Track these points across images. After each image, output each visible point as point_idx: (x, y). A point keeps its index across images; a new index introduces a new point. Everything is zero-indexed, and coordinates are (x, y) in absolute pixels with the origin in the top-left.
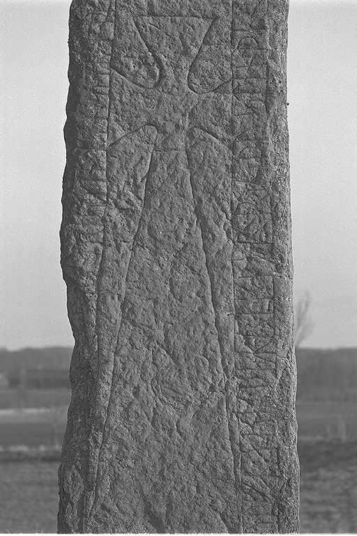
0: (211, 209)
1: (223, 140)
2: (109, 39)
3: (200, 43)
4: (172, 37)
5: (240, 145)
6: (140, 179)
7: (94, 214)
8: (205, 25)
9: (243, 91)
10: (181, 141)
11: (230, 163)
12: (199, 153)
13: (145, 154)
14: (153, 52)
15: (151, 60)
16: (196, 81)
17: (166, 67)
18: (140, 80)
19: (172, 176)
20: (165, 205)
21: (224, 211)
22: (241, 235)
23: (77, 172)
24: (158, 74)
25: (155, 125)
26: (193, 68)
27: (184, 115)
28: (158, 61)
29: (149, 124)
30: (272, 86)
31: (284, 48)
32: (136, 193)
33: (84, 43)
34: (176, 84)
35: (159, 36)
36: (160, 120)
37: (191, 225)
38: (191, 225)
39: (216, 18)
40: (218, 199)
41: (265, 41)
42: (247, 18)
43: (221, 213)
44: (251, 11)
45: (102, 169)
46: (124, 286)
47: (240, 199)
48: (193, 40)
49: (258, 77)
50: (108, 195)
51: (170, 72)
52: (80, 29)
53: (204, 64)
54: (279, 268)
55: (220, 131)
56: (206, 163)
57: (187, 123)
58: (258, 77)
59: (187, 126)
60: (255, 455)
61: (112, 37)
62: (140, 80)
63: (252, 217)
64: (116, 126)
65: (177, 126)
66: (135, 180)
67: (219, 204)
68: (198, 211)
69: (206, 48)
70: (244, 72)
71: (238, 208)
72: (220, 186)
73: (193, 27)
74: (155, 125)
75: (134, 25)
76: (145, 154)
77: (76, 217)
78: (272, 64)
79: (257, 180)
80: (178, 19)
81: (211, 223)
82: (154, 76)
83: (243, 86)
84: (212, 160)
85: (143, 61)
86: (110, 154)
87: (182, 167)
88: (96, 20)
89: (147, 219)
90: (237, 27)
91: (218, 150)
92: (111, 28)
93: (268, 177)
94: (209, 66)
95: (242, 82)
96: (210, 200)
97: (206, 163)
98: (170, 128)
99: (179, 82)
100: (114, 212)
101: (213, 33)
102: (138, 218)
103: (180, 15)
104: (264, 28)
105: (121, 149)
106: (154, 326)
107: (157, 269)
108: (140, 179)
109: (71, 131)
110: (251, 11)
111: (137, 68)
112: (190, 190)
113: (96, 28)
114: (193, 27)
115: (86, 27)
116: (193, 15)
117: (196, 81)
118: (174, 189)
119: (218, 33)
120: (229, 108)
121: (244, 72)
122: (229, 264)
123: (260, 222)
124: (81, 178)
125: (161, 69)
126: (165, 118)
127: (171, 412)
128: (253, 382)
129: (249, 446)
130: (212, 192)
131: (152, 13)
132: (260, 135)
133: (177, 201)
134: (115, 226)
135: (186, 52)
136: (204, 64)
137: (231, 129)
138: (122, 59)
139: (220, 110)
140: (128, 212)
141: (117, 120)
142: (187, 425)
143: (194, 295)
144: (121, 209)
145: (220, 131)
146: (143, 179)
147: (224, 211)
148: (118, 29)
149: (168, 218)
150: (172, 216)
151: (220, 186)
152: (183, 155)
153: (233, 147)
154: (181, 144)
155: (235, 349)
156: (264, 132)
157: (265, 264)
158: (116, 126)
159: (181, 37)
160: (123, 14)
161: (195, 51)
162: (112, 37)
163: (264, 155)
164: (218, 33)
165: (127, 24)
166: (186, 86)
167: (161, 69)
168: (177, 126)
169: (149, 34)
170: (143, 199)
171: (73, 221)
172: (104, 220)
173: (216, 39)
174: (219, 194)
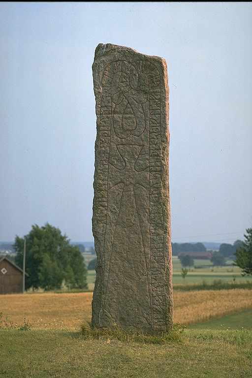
12: (138, 192)
15: (122, 160)
21: (147, 212)
22: (151, 220)
31: (168, 156)
46: (113, 238)
48: (136, 153)
53: (140, 161)
54: (165, 233)
60: (157, 298)
64: (110, 183)
69: (140, 156)
80: (131, 146)
81: (142, 217)
94: (141, 162)
106: (123, 253)
107: (124, 233)
122: (148, 231)
127: (129, 283)
128: (157, 272)
129: (155, 295)
130: (142, 206)
142: (134, 288)
143: (136, 242)
147: (147, 212)
155: (150, 261)
157: (161, 232)
166: (134, 170)
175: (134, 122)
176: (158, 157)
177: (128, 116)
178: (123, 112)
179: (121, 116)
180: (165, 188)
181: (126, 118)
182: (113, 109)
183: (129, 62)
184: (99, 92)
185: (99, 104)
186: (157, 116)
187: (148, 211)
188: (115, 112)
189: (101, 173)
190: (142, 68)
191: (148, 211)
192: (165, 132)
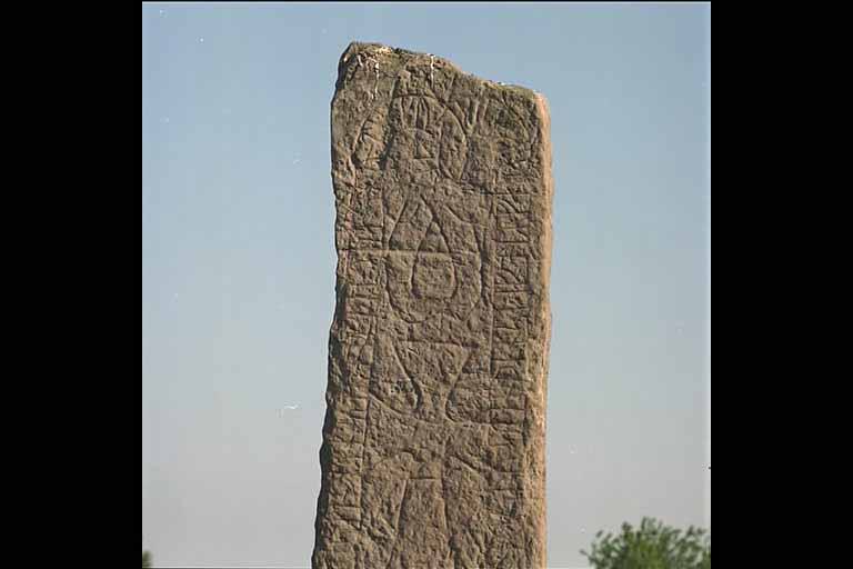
0: (465, 541)
1: (480, 470)
2: (367, 364)
3: (459, 370)
4: (430, 363)
5: (496, 475)
6: (394, 506)
7: (346, 541)
8: (465, 351)
9: (499, 422)
10: (436, 468)
11: (485, 494)
12: (454, 482)
13: (399, 481)
14: (412, 378)
16: (454, 409)
17: (423, 394)
18: (398, 406)
19: (427, 505)
20: (418, 535)
21: (477, 543)
23: (331, 497)
24: (416, 400)
25: (411, 451)
26: (451, 396)
27: (440, 443)
28: (416, 387)
29: (405, 451)
30: (530, 418)
32: (389, 521)
33: (342, 364)
34: (434, 411)
35: (418, 362)
36: (416, 447)
37: (444, 557)
38: (444, 557)
39: (475, 345)
40: (470, 531)
41: (524, 372)
42: (506, 347)
43: (475, 546)
44: (512, 340)
45: (356, 494)
47: (494, 532)
48: (452, 367)
49: (515, 407)
50: (361, 523)
51: (427, 398)
52: (340, 353)
53: (462, 391)
55: (476, 461)
56: (462, 493)
57: (444, 451)
58: (515, 407)
59: (443, 456)
61: (371, 360)
62: (398, 406)
63: (505, 551)
64: (372, 451)
65: (433, 454)
66: (389, 505)
67: (473, 535)
68: (451, 543)
70: (502, 401)
71: (492, 542)
72: (475, 518)
73: (453, 355)
74: (411, 451)
75: (393, 349)
76: (399, 481)
77: (329, 544)
78: (530, 394)
79: (513, 513)
80: (438, 345)
81: (464, 555)
82: (411, 402)
83: (501, 416)
84: (467, 490)
85: (402, 387)
86: (365, 479)
87: (437, 496)
88: (356, 343)
89: (400, 549)
90: (496, 357)
91: (473, 480)
92: (369, 351)
93: (523, 511)
95: (499, 412)
96: (464, 532)
97: (462, 493)
98: (426, 455)
99: (436, 409)
100: (367, 541)
101: (473, 361)
102: (390, 546)
103: (441, 342)
104: (523, 358)
105: (376, 475)
108: (394, 506)
109: (326, 454)
110: (512, 340)
111: (395, 393)
112: (443, 519)
113: (356, 350)
114: (453, 355)
115: (345, 350)
116: (454, 343)
117: (454, 409)
118: (428, 519)
119: (478, 362)
120: (485, 437)
121: (502, 401)
123: (514, 557)
124: (335, 504)
125: (420, 395)
126: (422, 447)
130: (467, 523)
131: (411, 339)
132: (516, 467)
133: (430, 530)
134: (367, 555)
135: (445, 381)
136: (462, 391)
137: (488, 459)
138: (380, 383)
139: (477, 441)
140: (381, 541)
141: (373, 446)
144: (374, 538)
145: (476, 461)
146: (397, 507)
147: (477, 543)
148: (377, 352)
149: (421, 550)
150: (425, 547)
151: (475, 518)
152: (438, 483)
153: (489, 478)
154: (436, 473)
156: (520, 465)
158: (372, 451)
159: (441, 364)
160: (382, 338)
161: (453, 378)
162: (371, 360)
163: (520, 488)
164: (478, 362)
165: (386, 348)
166: (444, 416)
167: (420, 395)
168: (433, 454)
169: (408, 359)
170: (396, 527)
171: (325, 547)
172: (356, 548)
173: (474, 367)
174: (473, 526)
175: (448, 277)
176: (517, 382)
177: (430, 256)
178: (416, 244)
179: (410, 256)
180: (534, 475)
181: (424, 263)
182: (388, 237)
183: (441, 101)
184: (349, 185)
185: (346, 220)
186: (517, 260)
187: (480, 538)
188: (394, 245)
189: (346, 421)
190: (478, 120)
191: (480, 538)
192: (539, 309)
